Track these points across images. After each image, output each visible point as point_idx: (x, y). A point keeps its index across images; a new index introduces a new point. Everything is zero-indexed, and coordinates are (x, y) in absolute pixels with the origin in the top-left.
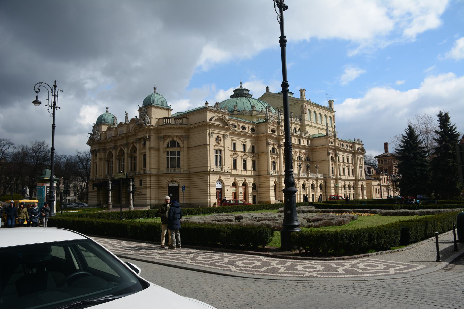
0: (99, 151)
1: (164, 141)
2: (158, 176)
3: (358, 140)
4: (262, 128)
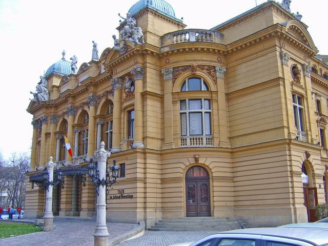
0: (45, 120)
1: (175, 79)
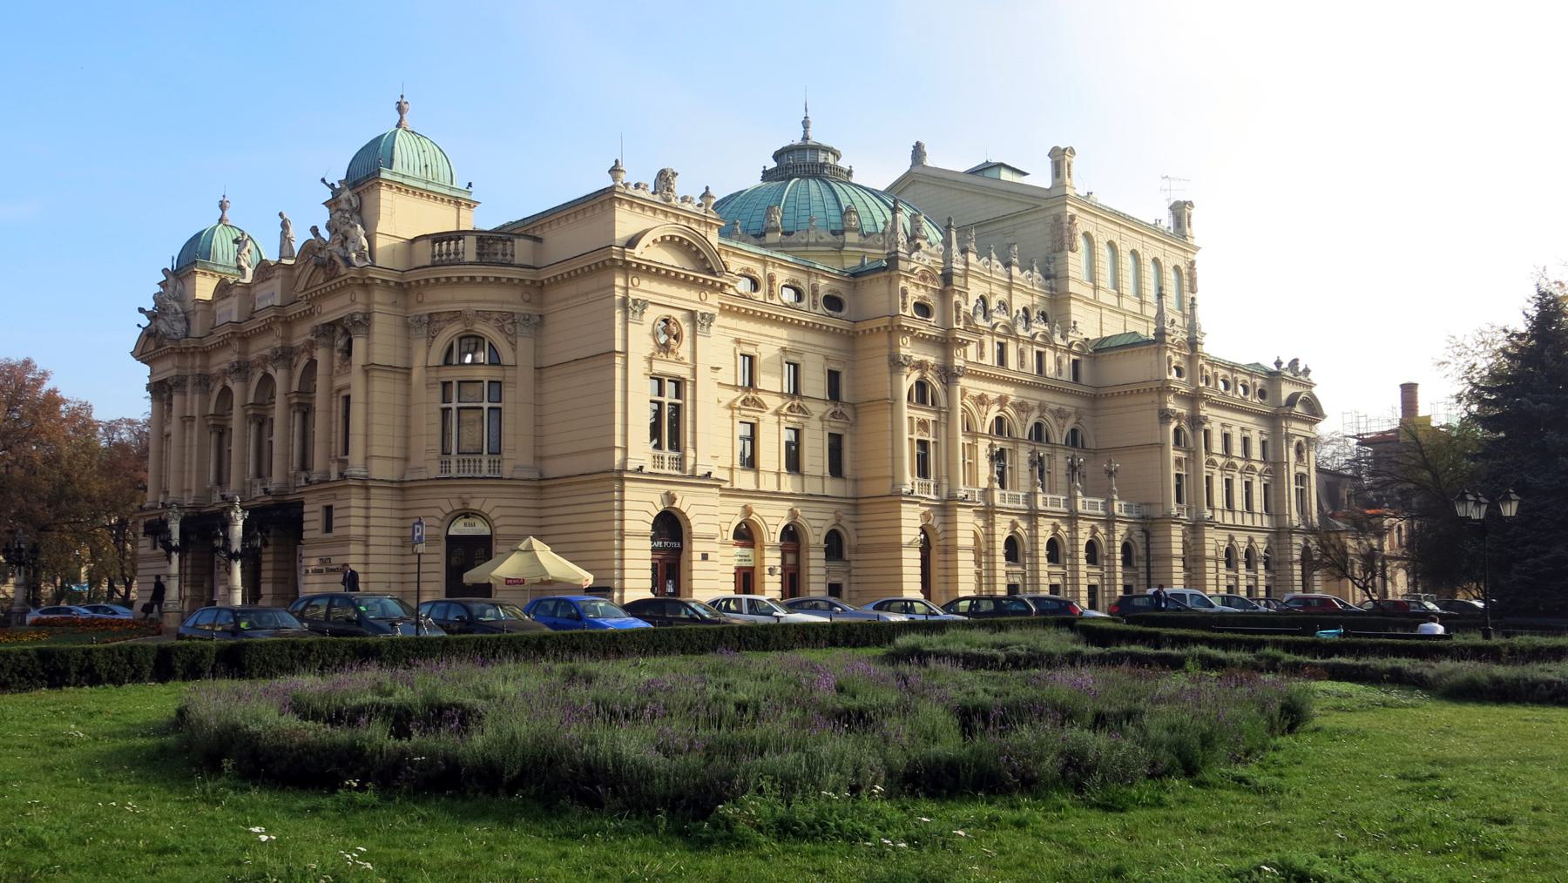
1: (432, 338)
2: (402, 488)
3: (1295, 362)
4: (875, 295)
